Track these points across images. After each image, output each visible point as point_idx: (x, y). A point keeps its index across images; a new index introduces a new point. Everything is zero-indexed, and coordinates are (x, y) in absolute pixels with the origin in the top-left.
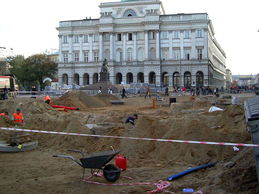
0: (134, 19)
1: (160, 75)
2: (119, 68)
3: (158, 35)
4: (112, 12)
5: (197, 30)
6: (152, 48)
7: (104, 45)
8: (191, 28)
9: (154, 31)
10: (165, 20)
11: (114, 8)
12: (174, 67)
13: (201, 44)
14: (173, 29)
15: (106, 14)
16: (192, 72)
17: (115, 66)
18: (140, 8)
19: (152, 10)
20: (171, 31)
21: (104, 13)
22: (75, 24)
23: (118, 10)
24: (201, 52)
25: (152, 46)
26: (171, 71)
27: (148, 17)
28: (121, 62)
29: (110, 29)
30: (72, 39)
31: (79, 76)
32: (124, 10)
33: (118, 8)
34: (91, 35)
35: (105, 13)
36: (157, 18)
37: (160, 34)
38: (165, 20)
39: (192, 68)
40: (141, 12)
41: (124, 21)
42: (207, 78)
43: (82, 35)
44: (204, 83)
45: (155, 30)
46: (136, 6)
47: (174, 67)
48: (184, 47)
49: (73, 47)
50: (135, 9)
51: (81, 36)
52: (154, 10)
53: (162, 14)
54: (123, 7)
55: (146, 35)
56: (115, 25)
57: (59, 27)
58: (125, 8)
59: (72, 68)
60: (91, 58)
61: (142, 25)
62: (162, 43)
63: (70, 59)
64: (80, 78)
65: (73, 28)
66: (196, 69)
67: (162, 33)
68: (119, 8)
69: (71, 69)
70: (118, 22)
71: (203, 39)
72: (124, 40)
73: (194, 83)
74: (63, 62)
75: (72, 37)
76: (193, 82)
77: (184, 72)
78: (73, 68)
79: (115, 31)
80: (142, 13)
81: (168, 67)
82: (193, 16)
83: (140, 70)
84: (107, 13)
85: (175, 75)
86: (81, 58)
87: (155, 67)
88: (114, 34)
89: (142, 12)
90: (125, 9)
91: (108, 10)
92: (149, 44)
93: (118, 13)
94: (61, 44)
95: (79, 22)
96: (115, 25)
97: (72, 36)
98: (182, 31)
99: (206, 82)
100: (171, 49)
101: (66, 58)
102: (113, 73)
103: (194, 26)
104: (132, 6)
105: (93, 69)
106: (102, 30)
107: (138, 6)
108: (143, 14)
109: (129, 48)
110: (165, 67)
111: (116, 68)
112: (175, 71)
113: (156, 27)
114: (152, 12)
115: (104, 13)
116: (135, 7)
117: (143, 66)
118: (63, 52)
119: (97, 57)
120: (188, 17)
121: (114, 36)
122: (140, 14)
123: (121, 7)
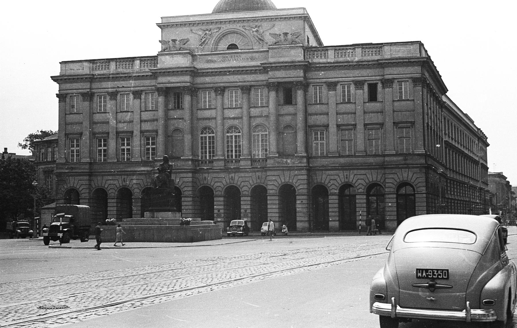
3: (300, 94)
4: (188, 40)
5: (396, 81)
12: (342, 171)
21: (169, 42)
30: (90, 104)
32: (218, 33)
37: (306, 91)
45: (293, 82)
47: (341, 173)
53: (313, 43)
57: (58, 74)
58: (220, 28)
62: (311, 115)
67: (311, 89)
69: (87, 178)
77: (340, 183)
79: (195, 86)
82: (386, 48)
83: (258, 181)
84: (177, 42)
85: (347, 192)
87: (293, 173)
89: (261, 40)
90: (220, 31)
91: (179, 34)
100: (333, 129)
104: (239, 24)
109: (230, 128)
112: (343, 181)
113: (298, 75)
117: (264, 169)
119: (153, 149)
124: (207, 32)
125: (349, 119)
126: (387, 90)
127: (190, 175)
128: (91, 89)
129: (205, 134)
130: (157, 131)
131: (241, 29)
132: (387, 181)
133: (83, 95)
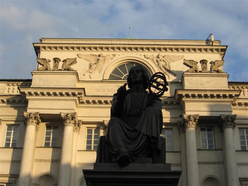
11: (83, 53)
15: (56, 66)
19: (203, 62)
21: (50, 61)
25: (211, 171)
27: (194, 78)
29: (66, 107)
33: (93, 55)
45: (220, 117)
50: (146, 59)
52: (211, 63)
54: (110, 53)
56: (83, 95)
58: (114, 55)
61: (172, 103)
68: (99, 56)
79: (79, 119)
84: (61, 64)
90: (115, 58)
107: (155, 54)
114: (204, 68)
115: (50, 61)
116: (148, 56)
121: (75, 134)
123: (105, 53)
131: (143, 58)
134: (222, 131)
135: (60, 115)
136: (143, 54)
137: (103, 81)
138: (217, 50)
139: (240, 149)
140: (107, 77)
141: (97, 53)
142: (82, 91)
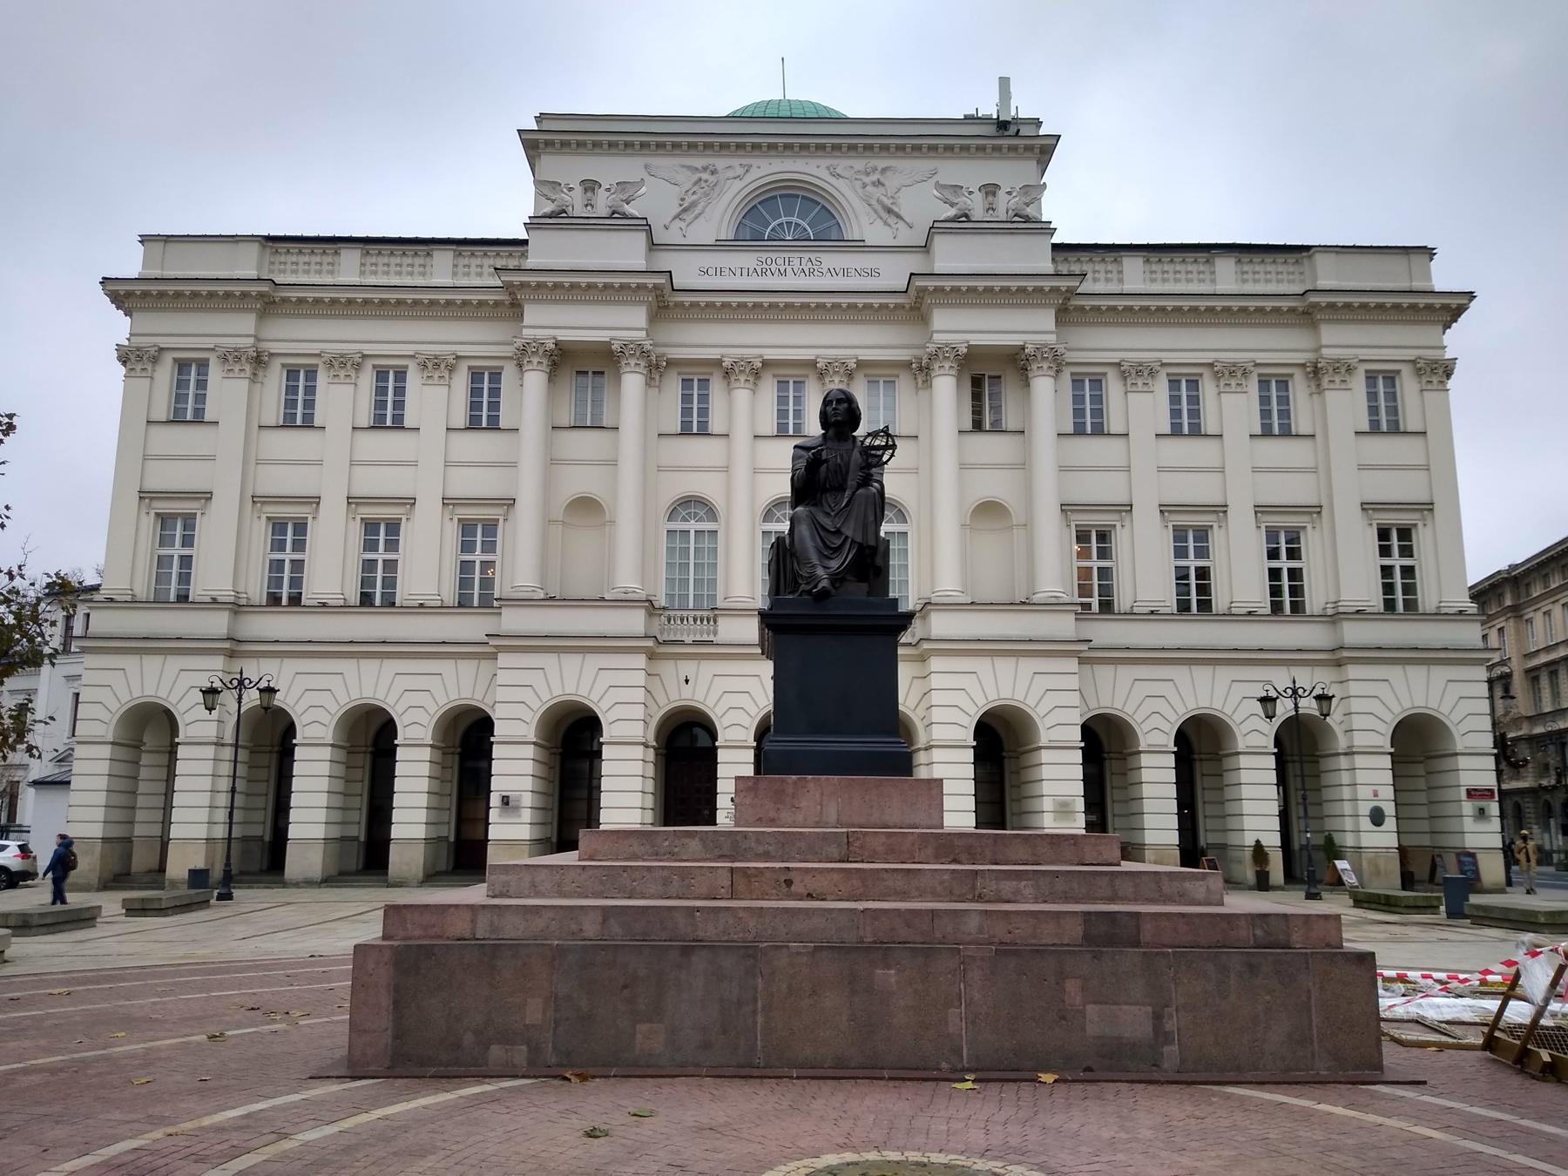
0: (830, 260)
1: (1077, 734)
2: (687, 668)
6: (989, 510)
7: (552, 461)
8: (1310, 356)
9: (1017, 362)
10: (1098, 281)
13: (1406, 488)
14: (1168, 357)
16: (1357, 722)
17: (657, 650)
18: (874, 177)
19: (990, 190)
20: (1136, 373)
21: (571, 189)
22: (295, 272)
23: (687, 179)
24: (1407, 551)
26: (1160, 705)
28: (714, 614)
31: (290, 729)
32: (738, 185)
33: (689, 168)
34: (439, 367)
35: (579, 190)
36: (1034, 258)
38: (1098, 281)
39: (1354, 688)
40: (890, 211)
41: (742, 271)
42: (1489, 780)
43: (358, 367)
44: (1469, 824)
45: (1023, 348)
46: (842, 164)
48: (1260, 510)
49: (251, 461)
51: (345, 364)
54: (735, 162)
55: (946, 387)
59: (231, 655)
60: (426, 562)
63: (212, 577)
64: (299, 753)
65: (269, 302)
66: (1381, 690)
68: (705, 169)
70: (688, 272)
71: (1417, 442)
72: (742, 436)
73: (1377, 817)
74: (142, 589)
75: (254, 378)
76: (1365, 808)
78: (234, 647)
79: (660, 350)
80: (898, 216)
81: (1127, 673)
82: (1320, 259)
86: (331, 565)
88: (656, 368)
92: (963, 466)
93: (694, 204)
94: (139, 426)
95: (336, 253)
96: (665, 302)
97: (259, 361)
98: (1228, 374)
99: (1482, 811)
101: (182, 557)
102: (639, 712)
103: (1337, 340)
105: (445, 667)
106: (548, 322)
107: (859, 164)
108: (901, 224)
110: (1104, 673)
111: (667, 669)
113: (1030, 327)
115: (571, 189)
118: (145, 496)
119: (486, 565)
120: (1270, 268)
122: (879, 223)
123: (720, 163)
124: (705, 176)
125: (1201, 490)
126: (1330, 396)
127: (640, 661)
128: (258, 339)
129: (684, 519)
130: (510, 503)
131: (825, 174)
132: (1356, 705)
133: (230, 357)
134: (1026, 384)
135: (609, 344)
136: (829, 162)
137: (719, 246)
138: (1029, 148)
139: (1070, 429)
140: (727, 233)
141: (699, 162)
142: (661, 280)
